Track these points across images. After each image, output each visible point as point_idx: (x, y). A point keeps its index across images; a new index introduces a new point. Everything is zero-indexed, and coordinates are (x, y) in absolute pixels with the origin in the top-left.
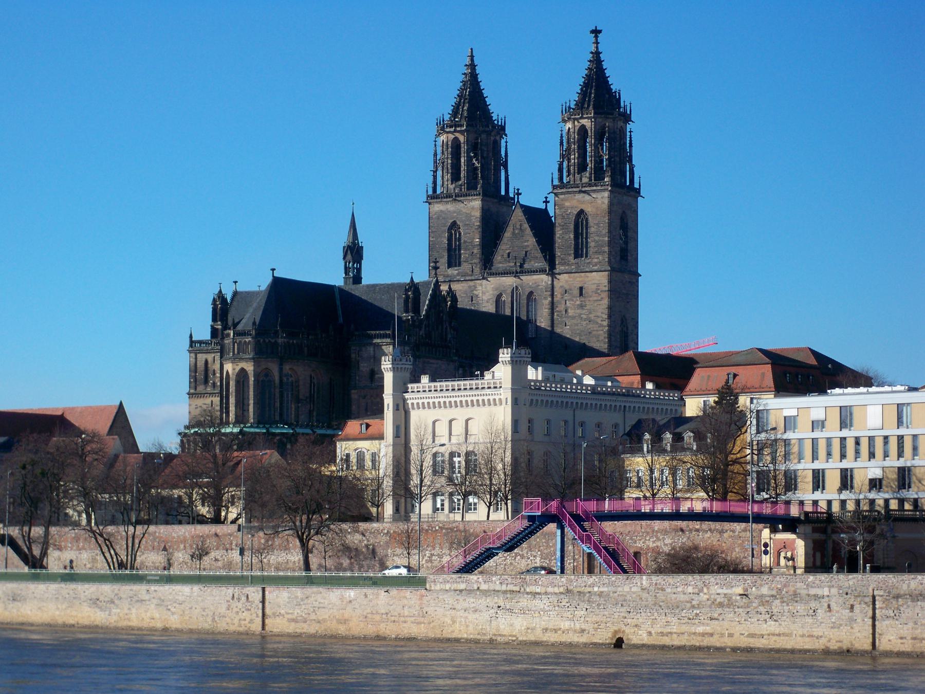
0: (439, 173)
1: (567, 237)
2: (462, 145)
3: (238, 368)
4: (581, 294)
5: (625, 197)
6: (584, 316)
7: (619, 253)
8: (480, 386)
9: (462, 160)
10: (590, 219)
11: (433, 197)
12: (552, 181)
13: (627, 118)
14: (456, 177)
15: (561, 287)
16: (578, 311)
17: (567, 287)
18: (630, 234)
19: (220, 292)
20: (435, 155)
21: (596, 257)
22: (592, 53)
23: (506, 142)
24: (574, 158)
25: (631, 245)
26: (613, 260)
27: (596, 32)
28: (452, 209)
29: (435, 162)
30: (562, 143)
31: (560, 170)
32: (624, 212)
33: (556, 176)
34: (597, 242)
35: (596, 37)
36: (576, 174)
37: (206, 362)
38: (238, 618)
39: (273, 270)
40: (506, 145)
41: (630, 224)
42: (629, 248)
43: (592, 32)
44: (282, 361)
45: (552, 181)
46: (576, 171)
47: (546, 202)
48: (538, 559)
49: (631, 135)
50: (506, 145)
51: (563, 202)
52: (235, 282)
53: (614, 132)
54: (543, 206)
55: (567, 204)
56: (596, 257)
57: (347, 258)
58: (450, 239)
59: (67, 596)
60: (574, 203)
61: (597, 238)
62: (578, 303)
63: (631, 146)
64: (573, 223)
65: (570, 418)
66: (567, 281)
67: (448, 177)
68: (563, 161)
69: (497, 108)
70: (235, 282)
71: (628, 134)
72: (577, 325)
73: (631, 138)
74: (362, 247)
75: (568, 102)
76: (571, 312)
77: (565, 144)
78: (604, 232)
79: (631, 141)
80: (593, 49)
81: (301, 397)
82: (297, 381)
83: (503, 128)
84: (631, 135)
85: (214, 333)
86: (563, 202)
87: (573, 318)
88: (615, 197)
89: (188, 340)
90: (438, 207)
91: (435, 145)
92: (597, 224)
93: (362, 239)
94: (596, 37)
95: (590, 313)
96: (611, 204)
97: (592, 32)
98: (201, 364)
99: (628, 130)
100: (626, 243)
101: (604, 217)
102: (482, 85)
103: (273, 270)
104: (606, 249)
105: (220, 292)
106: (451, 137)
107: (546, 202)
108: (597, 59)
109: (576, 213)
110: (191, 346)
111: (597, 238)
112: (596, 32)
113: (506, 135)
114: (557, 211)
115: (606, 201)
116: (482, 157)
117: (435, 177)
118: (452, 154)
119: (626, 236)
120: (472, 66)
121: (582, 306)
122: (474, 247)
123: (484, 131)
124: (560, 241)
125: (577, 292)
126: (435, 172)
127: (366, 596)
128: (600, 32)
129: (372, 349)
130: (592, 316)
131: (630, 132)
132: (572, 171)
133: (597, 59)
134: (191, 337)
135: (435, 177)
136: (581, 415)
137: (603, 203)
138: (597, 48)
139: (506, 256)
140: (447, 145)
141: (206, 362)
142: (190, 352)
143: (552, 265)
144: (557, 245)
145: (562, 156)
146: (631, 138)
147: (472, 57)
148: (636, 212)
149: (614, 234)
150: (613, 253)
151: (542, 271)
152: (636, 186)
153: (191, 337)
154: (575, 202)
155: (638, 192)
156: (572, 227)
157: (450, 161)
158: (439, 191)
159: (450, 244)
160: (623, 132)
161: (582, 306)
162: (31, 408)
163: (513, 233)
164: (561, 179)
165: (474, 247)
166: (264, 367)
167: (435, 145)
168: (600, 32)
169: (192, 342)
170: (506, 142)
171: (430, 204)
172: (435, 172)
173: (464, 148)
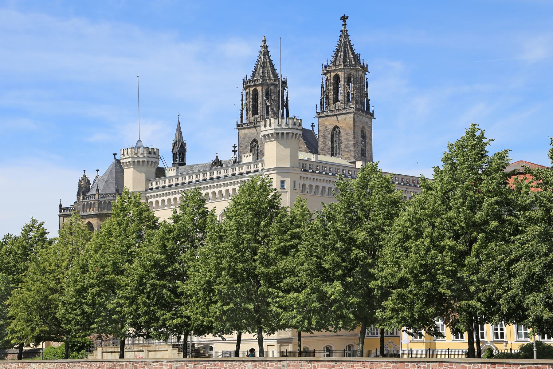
0: (245, 111)
1: (327, 143)
2: (259, 93)
5: (364, 118)
7: (360, 152)
9: (259, 102)
10: (341, 131)
11: (240, 126)
12: (317, 110)
14: (255, 112)
18: (367, 141)
19: (85, 176)
20: (242, 101)
21: (346, 154)
23: (287, 92)
24: (331, 95)
25: (368, 148)
26: (357, 156)
28: (253, 132)
30: (322, 86)
31: (322, 103)
32: (363, 127)
34: (346, 145)
36: (332, 105)
40: (287, 94)
41: (367, 135)
42: (367, 149)
45: (317, 110)
46: (332, 103)
47: (313, 126)
49: (367, 81)
50: (287, 94)
51: (324, 122)
52: (98, 171)
53: (357, 78)
54: (311, 129)
55: (326, 123)
56: (346, 154)
57: (174, 151)
61: (346, 143)
63: (367, 87)
64: (330, 134)
67: (250, 113)
68: (323, 98)
70: (98, 171)
71: (366, 80)
73: (367, 82)
74: (185, 143)
75: (326, 61)
77: (324, 87)
78: (351, 139)
79: (367, 84)
84: (367, 81)
86: (324, 122)
88: (358, 117)
89: (59, 208)
90: (243, 132)
91: (242, 95)
92: (347, 134)
93: (186, 138)
96: (355, 121)
99: (366, 78)
101: (351, 129)
104: (353, 149)
105: (85, 176)
107: (313, 126)
109: (332, 128)
110: (61, 212)
111: (346, 143)
114: (320, 128)
115: (352, 119)
116: (272, 99)
117: (242, 114)
118: (252, 99)
119: (365, 142)
124: (322, 146)
126: (242, 111)
131: (367, 79)
132: (330, 103)
134: (61, 205)
135: (242, 114)
137: (350, 121)
142: (60, 216)
144: (320, 149)
146: (367, 82)
148: (371, 127)
149: (357, 139)
150: (357, 151)
152: (371, 111)
153: (61, 205)
154: (331, 122)
155: (372, 115)
156: (330, 137)
157: (251, 103)
158: (245, 122)
160: (362, 79)
164: (322, 108)
167: (242, 95)
169: (61, 208)
170: (287, 92)
171: (239, 129)
173: (260, 94)
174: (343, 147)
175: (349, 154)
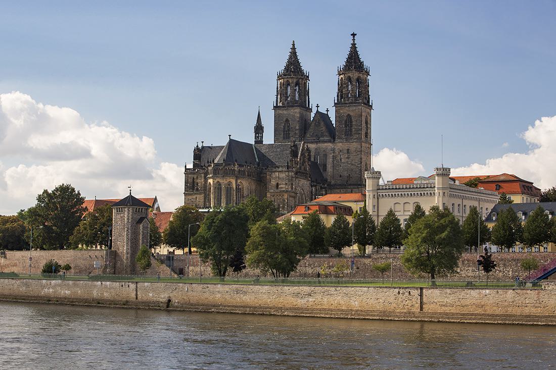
0: (279, 96)
3: (216, 181)
4: (348, 152)
6: (350, 162)
8: (391, 188)
11: (276, 108)
13: (368, 74)
15: (338, 149)
16: (347, 160)
17: (341, 149)
18: (368, 126)
20: (277, 88)
22: (352, 44)
25: (369, 131)
27: (354, 35)
29: (277, 91)
30: (338, 84)
33: (336, 99)
35: (354, 37)
37: (194, 179)
38: (402, 304)
39: (230, 136)
41: (369, 122)
43: (352, 35)
44: (237, 178)
48: (510, 273)
52: (203, 142)
58: (284, 127)
59: (276, 292)
60: (345, 111)
61: (356, 127)
62: (346, 156)
65: (461, 204)
66: (341, 146)
69: (305, 67)
70: (203, 142)
72: (346, 166)
76: (343, 160)
80: (352, 42)
81: (244, 195)
82: (243, 188)
83: (308, 77)
85: (195, 165)
87: (344, 163)
92: (356, 121)
94: (354, 37)
95: (352, 161)
97: (352, 35)
98: (190, 180)
100: (367, 130)
102: (298, 58)
103: (230, 136)
105: (197, 146)
106: (286, 80)
108: (354, 45)
110: (186, 171)
111: (356, 127)
112: (354, 35)
113: (309, 80)
120: (294, 48)
121: (348, 158)
122: (296, 130)
123: (301, 78)
125: (346, 151)
126: (277, 96)
127: (498, 292)
128: (356, 35)
129: (277, 173)
130: (353, 163)
133: (354, 45)
134: (186, 166)
135: (277, 98)
136: (466, 202)
138: (354, 41)
139: (311, 134)
140: (283, 84)
141: (194, 179)
143: (334, 139)
145: (339, 90)
147: (294, 45)
151: (330, 142)
153: (186, 166)
154: (345, 111)
155: (371, 106)
159: (284, 128)
161: (348, 158)
162: (510, 172)
163: (315, 124)
165: (296, 130)
166: (228, 181)
168: (356, 35)
172: (277, 96)
174: (353, 130)
175: (357, 136)
